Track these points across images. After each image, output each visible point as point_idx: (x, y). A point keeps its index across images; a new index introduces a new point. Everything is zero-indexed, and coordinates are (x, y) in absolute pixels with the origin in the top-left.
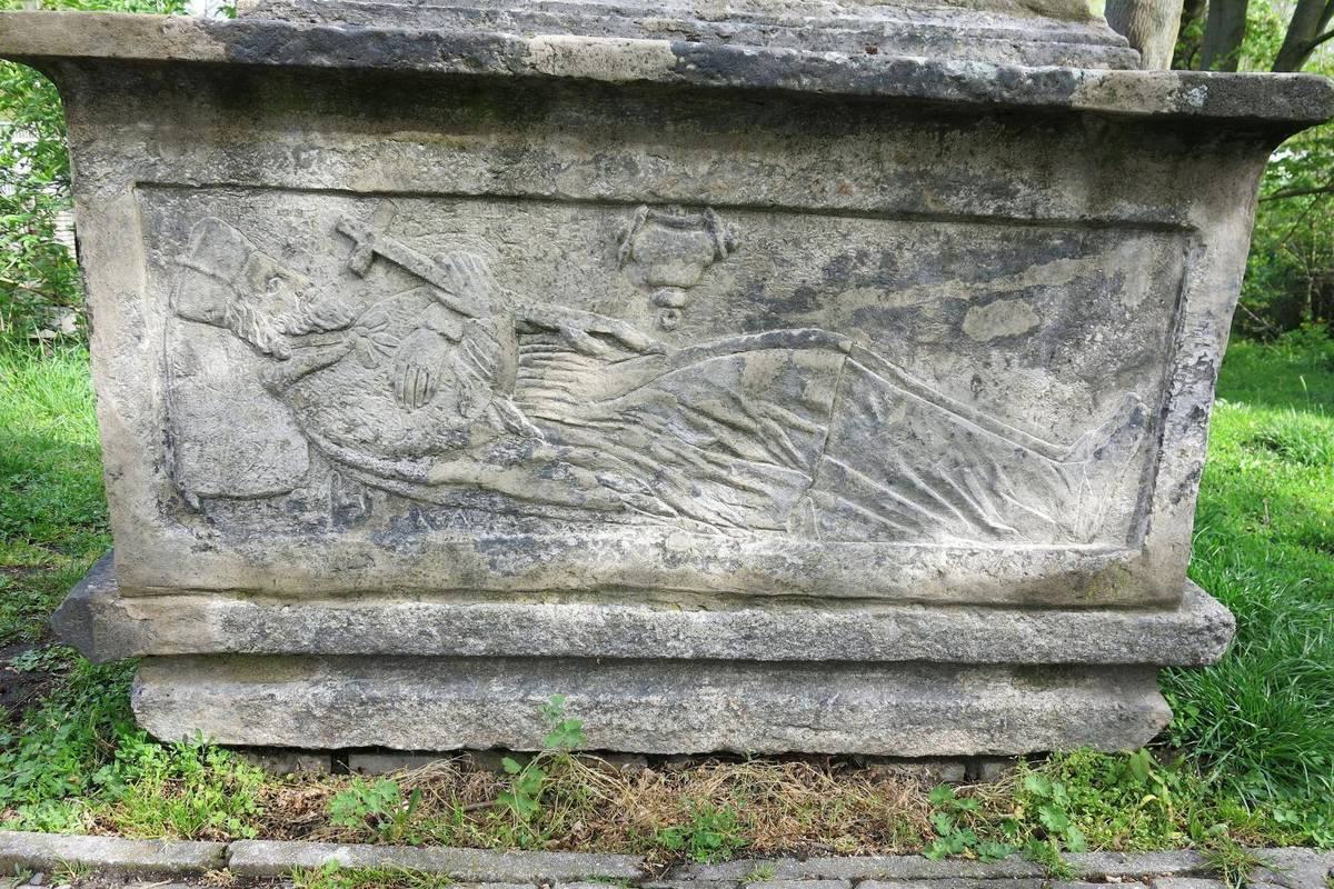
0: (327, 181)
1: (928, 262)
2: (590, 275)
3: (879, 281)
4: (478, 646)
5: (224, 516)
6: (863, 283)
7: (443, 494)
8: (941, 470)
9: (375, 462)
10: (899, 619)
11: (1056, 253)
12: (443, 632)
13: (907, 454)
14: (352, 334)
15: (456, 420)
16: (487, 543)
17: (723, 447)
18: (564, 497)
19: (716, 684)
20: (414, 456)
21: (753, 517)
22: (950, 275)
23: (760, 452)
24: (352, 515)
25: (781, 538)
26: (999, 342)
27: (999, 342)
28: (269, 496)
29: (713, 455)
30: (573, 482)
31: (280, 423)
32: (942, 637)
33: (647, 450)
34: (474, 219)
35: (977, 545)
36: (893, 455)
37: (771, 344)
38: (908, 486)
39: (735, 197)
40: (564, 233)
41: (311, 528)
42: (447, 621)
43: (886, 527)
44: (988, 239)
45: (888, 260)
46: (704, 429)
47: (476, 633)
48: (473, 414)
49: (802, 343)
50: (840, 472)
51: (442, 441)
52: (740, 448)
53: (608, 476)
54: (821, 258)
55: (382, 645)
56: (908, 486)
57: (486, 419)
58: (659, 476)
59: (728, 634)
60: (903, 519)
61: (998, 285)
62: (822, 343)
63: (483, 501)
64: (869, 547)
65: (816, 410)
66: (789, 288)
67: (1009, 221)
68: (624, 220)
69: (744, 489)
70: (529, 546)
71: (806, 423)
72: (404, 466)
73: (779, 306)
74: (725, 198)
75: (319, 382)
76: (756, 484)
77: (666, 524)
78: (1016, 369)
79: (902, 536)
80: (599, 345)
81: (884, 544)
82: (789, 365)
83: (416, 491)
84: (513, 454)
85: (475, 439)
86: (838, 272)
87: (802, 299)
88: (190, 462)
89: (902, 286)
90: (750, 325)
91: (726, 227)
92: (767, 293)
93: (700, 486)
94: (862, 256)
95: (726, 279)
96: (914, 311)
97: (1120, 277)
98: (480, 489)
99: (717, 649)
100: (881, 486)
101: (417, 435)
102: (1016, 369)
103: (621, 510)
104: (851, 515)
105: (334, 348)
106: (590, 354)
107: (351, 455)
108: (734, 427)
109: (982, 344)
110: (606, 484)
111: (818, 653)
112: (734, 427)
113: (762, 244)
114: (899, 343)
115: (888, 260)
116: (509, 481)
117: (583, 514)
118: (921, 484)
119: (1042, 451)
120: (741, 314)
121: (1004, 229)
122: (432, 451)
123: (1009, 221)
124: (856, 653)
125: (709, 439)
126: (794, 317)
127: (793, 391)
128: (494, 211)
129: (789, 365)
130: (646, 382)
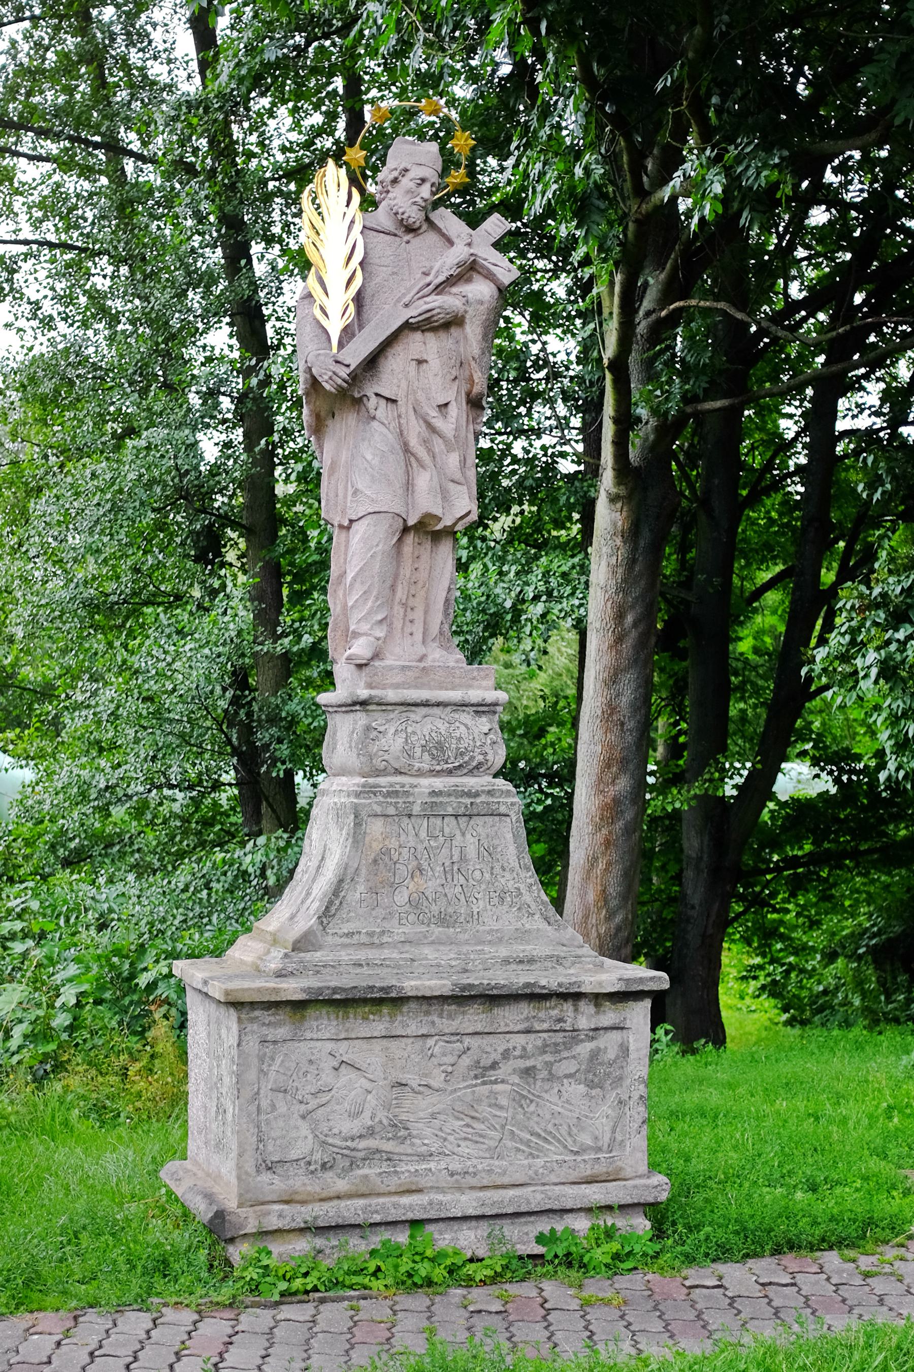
0: (328, 1036)
1: (537, 1047)
2: (418, 1063)
3: (521, 1057)
4: (377, 1218)
5: (279, 1170)
6: (515, 1058)
7: (361, 1155)
8: (550, 1127)
9: (338, 1142)
10: (542, 1192)
11: (582, 1041)
12: (364, 1213)
13: (537, 1123)
14: (333, 1092)
15: (370, 1123)
16: (380, 1174)
17: (468, 1126)
18: (410, 1151)
19: (469, 1229)
20: (353, 1139)
21: (481, 1154)
22: (545, 1052)
23: (483, 1127)
24: (329, 1165)
25: (492, 1162)
26: (567, 1076)
27: (567, 1076)
28: (297, 1160)
29: (464, 1129)
30: (413, 1144)
31: (304, 1129)
32: (557, 1198)
33: (441, 1129)
34: (377, 1045)
35: (567, 1158)
36: (532, 1123)
37: (484, 1083)
38: (539, 1136)
39: (470, 1031)
40: (409, 1048)
41: (312, 1172)
42: (364, 1209)
43: (531, 1154)
44: (559, 1038)
45: (524, 1049)
46: (462, 1119)
47: (377, 1212)
48: (377, 1120)
49: (496, 1082)
50: (512, 1132)
51: (364, 1132)
52: (475, 1126)
53: (426, 1141)
54: (501, 1050)
55: (340, 1222)
56: (539, 1136)
57: (381, 1122)
58: (445, 1140)
59: (475, 1204)
60: (537, 1150)
61: (565, 1054)
62: (503, 1082)
63: (377, 1156)
64: (526, 1162)
65: (501, 1108)
66: (489, 1062)
67: (565, 1031)
68: (430, 1042)
69: (477, 1142)
70: (396, 1172)
71: (498, 1113)
72: (349, 1143)
73: (486, 1069)
74: (467, 1031)
75: (320, 1111)
76: (481, 1140)
77: (448, 1159)
78: (573, 1085)
79: (538, 1157)
80: (421, 1088)
81: (530, 1160)
82: (491, 1092)
83: (353, 1154)
84: (390, 1135)
85: (377, 1130)
86: (506, 1055)
87: (494, 1066)
88: (270, 1148)
89: (529, 1058)
90: (476, 1077)
91: (467, 1040)
92: (482, 1065)
93: (460, 1143)
94: (514, 1048)
95: (466, 1061)
96: (534, 1067)
97: (606, 1048)
98: (378, 1151)
99: (471, 1212)
100: (529, 1137)
101: (355, 1131)
102: (573, 1085)
103: (431, 1155)
104: (518, 1150)
105: (324, 1098)
106: (419, 1093)
107: (330, 1140)
108: (473, 1118)
109: (558, 1078)
110: (425, 1145)
111: (510, 1210)
112: (473, 1118)
113: (479, 1047)
114: (531, 1080)
115: (524, 1049)
116: (388, 1146)
117: (417, 1158)
118: (543, 1134)
119: (587, 1117)
120: (472, 1073)
121: (564, 1034)
122: (360, 1137)
123: (565, 1031)
124: (524, 1208)
125: (463, 1123)
126: (492, 1072)
127: (493, 1101)
128: (385, 1042)
129: (491, 1092)
130: (439, 1102)
